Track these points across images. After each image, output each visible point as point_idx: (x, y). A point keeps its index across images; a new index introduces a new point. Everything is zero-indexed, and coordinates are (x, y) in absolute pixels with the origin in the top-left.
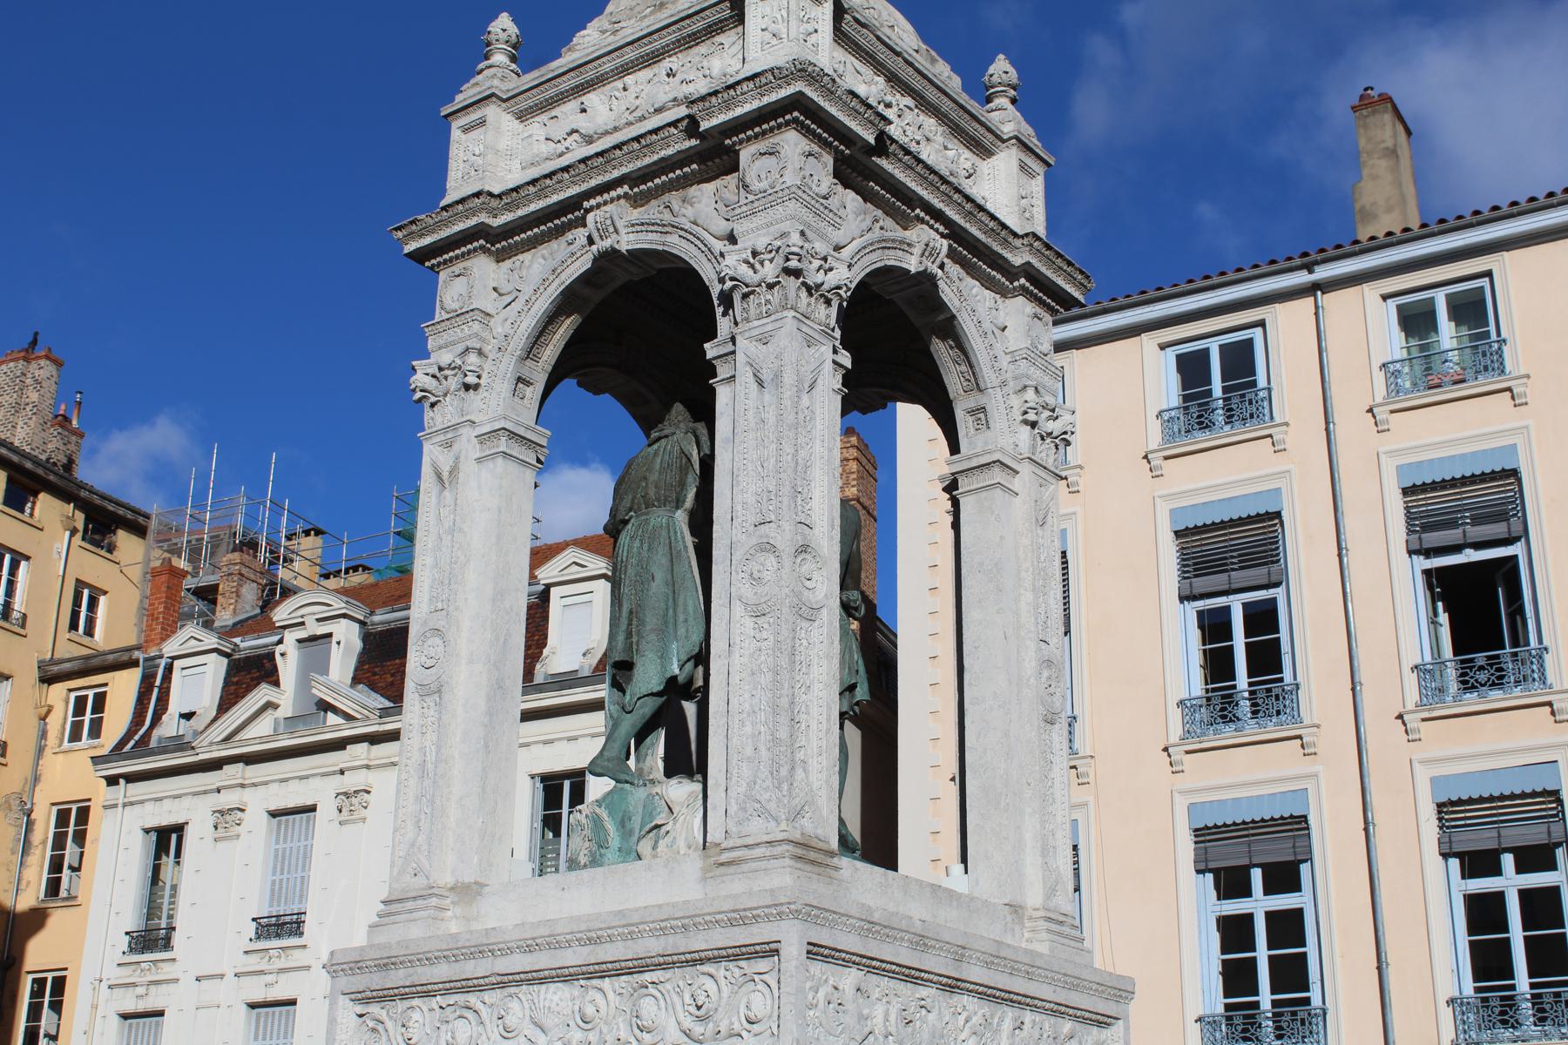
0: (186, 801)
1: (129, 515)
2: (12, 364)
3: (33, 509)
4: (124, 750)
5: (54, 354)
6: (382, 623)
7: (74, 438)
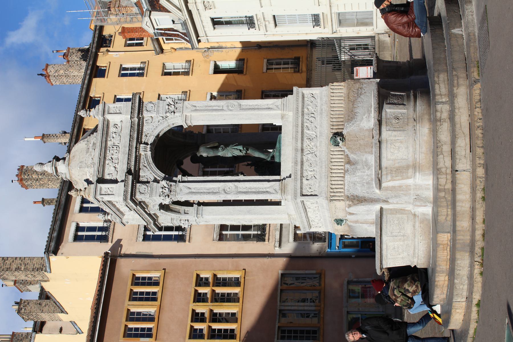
0: (203, 18)
1: (97, 32)
2: (52, 81)
3: (103, 67)
4: (188, 40)
5: (44, 67)
7: (71, 51)
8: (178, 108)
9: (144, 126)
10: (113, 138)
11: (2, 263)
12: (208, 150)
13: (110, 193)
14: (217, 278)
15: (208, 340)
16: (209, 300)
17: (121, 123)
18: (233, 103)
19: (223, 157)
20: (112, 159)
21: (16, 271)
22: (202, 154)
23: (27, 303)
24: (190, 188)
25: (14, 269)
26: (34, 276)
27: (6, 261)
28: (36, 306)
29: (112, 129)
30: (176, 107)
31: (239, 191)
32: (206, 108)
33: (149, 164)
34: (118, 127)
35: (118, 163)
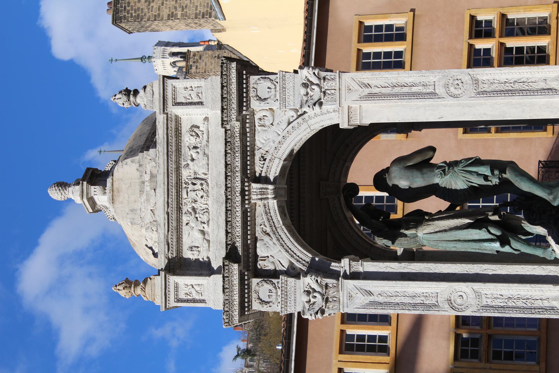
8: (328, 92)
9: (256, 133)
10: (193, 160)
11: (146, 8)
12: (409, 173)
13: (197, 297)
14: (507, 20)
15: (496, 134)
16: (496, 62)
17: (206, 123)
18: (458, 78)
19: (445, 188)
20: (196, 213)
21: (169, 19)
22: (396, 182)
23: (198, 56)
24: (370, 293)
25: (165, 17)
26: (200, 25)
27: (152, 4)
28: (213, 61)
29: (187, 140)
30: (323, 90)
31: (485, 303)
32: (397, 90)
33: (273, 225)
34: (200, 133)
35: (208, 221)
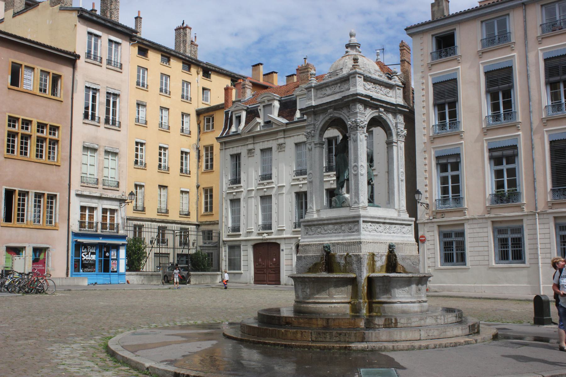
1: (214, 68)
6: (284, 100)
